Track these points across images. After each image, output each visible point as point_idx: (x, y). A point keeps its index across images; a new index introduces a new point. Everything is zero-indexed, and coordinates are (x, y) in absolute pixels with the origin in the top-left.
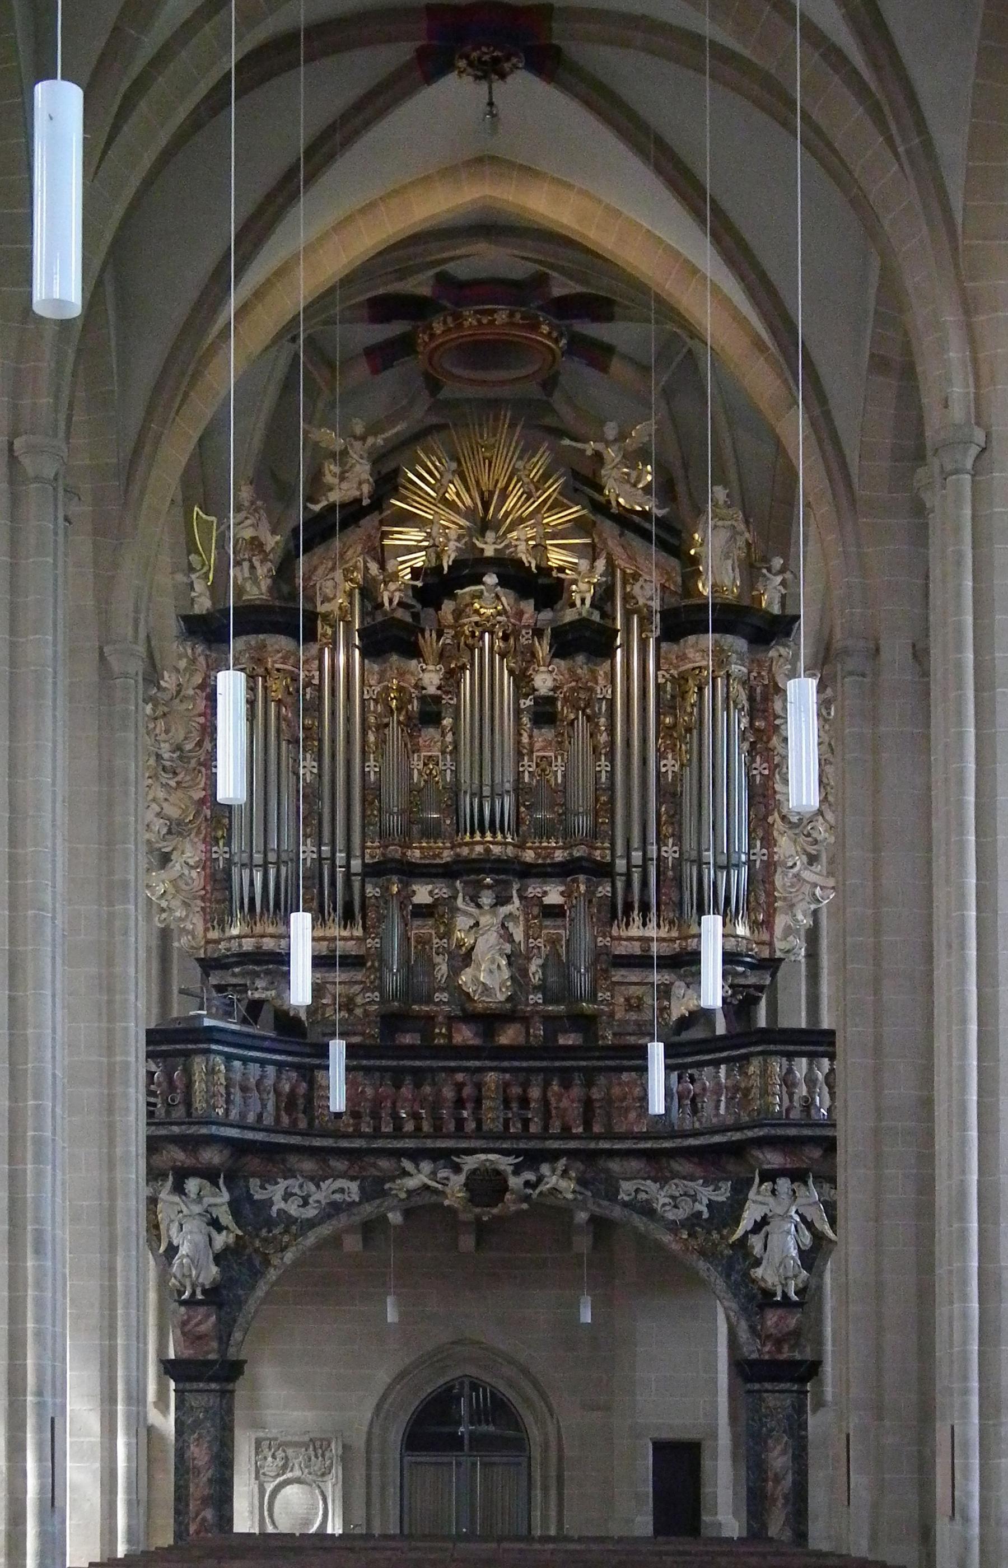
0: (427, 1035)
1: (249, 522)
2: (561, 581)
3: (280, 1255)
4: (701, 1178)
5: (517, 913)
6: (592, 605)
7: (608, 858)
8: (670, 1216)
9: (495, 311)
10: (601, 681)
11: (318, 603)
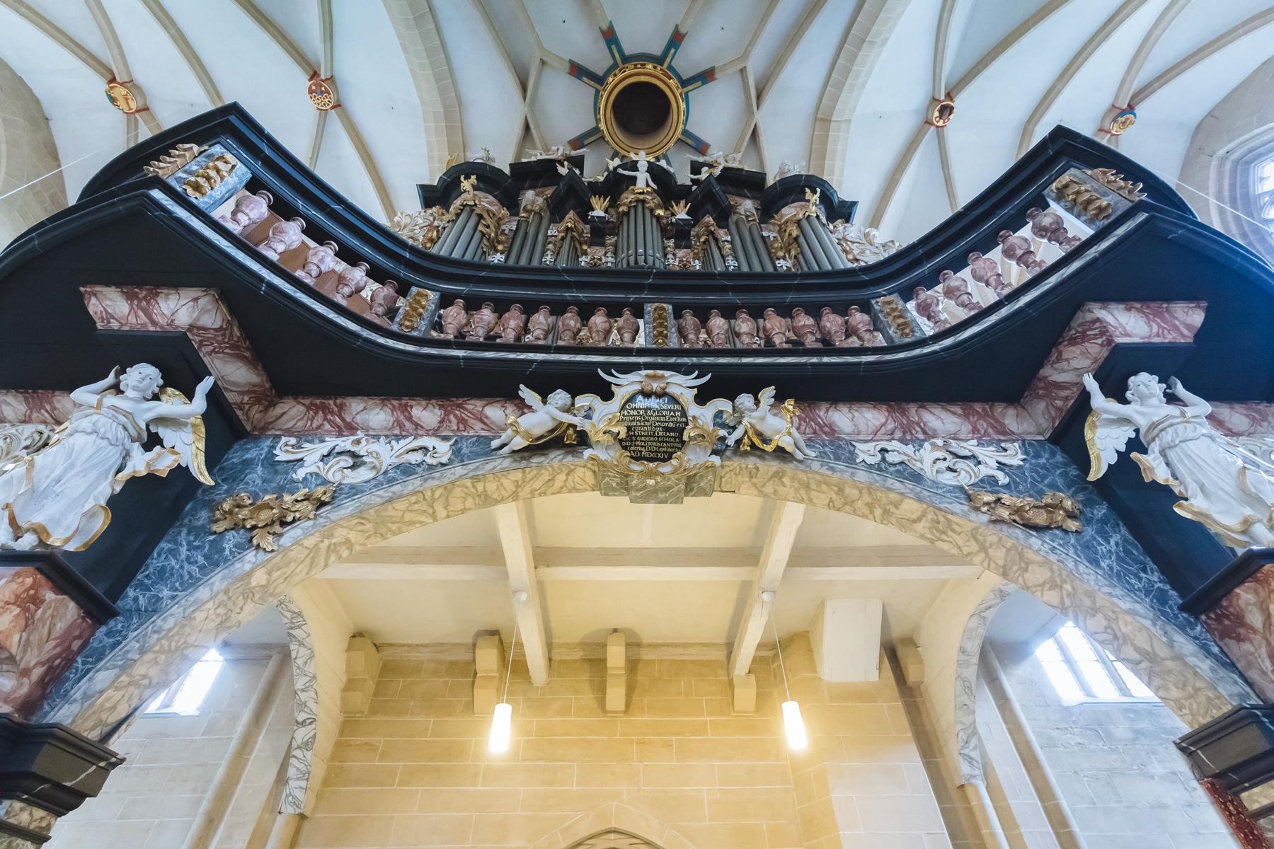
3: (277, 529)
8: (948, 479)
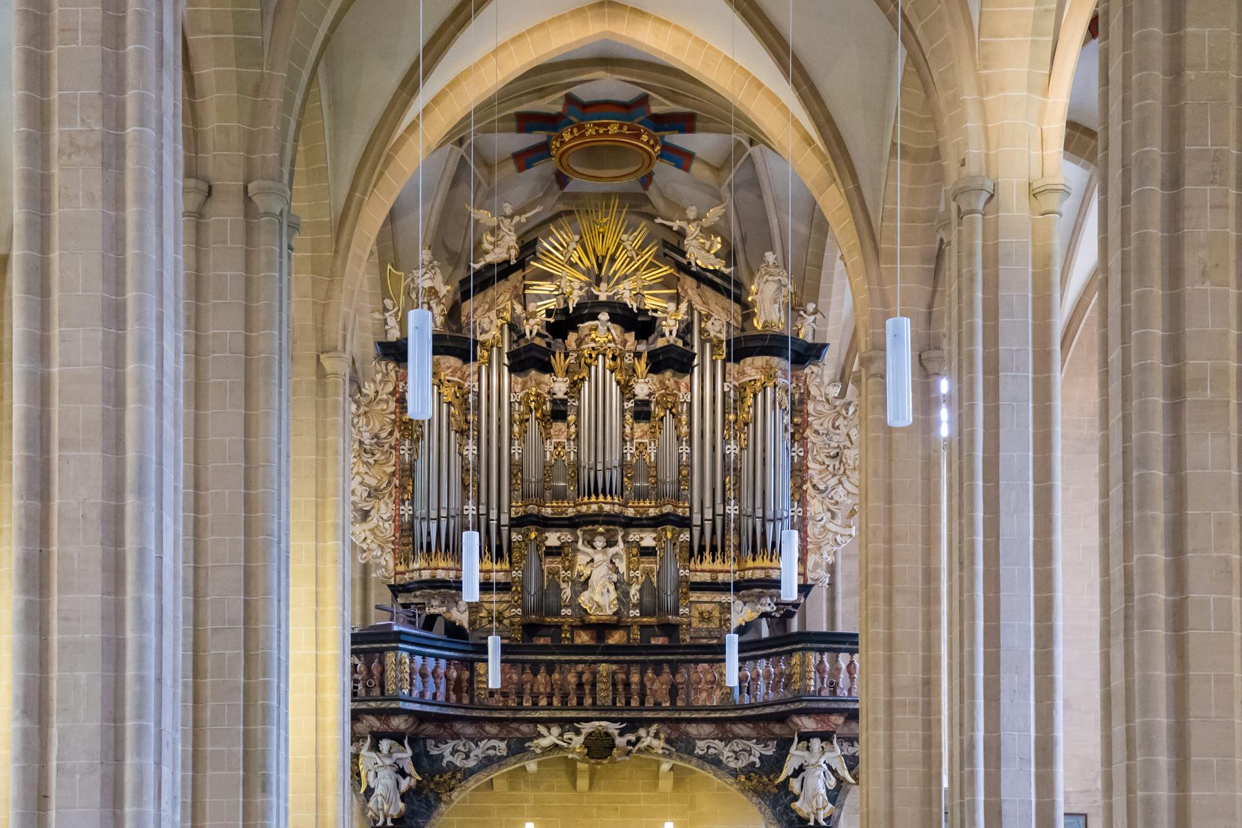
0: (556, 637)
1: (427, 276)
2: (655, 319)
3: (448, 794)
4: (753, 739)
5: (622, 553)
6: (677, 336)
7: (688, 514)
8: (732, 765)
9: (608, 124)
10: (683, 389)
11: (478, 334)
